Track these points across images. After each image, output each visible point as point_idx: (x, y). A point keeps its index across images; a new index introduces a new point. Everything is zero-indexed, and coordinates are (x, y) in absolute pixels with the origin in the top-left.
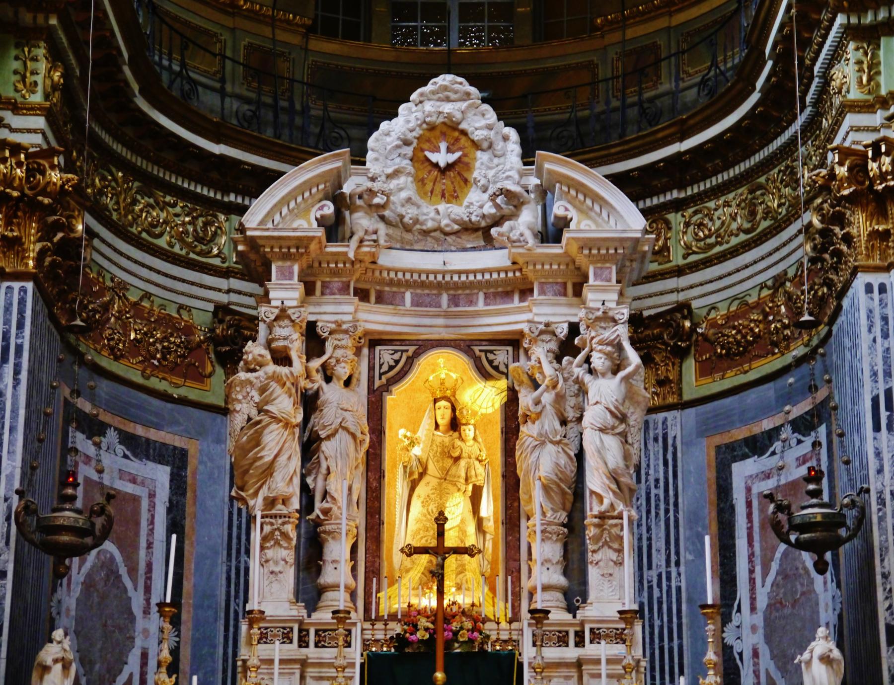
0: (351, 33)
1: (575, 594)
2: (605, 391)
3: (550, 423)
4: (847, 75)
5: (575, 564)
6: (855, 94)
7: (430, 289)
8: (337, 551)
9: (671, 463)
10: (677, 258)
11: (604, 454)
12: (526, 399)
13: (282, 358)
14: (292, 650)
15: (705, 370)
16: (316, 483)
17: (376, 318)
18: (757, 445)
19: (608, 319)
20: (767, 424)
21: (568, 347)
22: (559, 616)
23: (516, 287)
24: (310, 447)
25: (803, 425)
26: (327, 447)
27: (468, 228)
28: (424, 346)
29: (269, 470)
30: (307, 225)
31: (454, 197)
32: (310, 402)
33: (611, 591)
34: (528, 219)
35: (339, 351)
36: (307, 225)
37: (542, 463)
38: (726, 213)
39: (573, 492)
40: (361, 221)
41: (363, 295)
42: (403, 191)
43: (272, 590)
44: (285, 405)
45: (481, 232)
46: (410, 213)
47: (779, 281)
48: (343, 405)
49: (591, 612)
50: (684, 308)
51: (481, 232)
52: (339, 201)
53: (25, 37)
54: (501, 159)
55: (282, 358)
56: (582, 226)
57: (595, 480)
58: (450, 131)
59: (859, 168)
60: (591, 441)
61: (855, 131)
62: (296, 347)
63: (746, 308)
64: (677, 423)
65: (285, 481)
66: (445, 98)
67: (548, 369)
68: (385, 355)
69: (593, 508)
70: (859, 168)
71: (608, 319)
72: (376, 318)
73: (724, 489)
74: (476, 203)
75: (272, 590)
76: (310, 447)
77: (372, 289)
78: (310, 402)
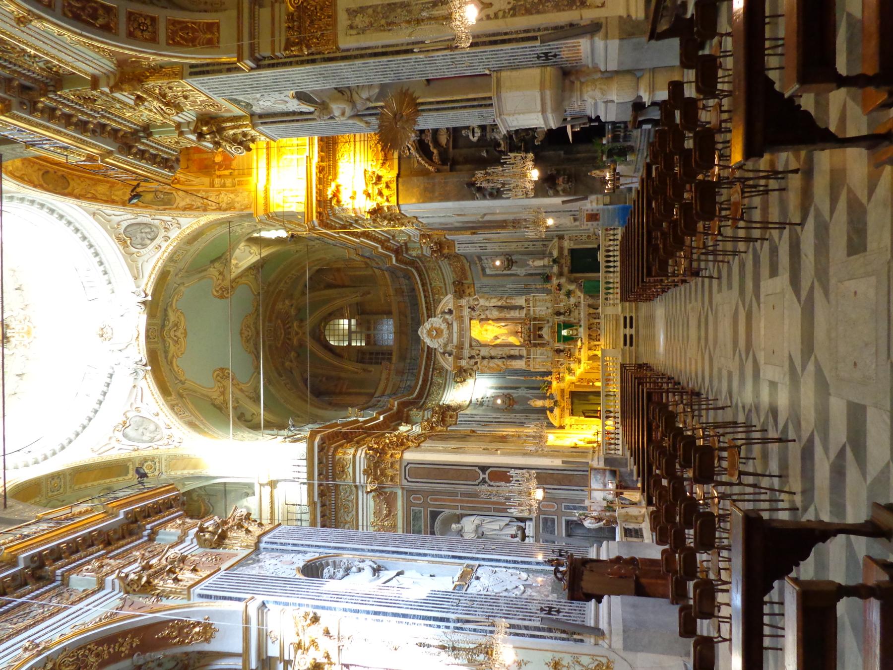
0: (391, 354)
1: (521, 308)
2: (482, 302)
3: (487, 312)
4: (414, 254)
5: (514, 308)
6: (419, 252)
7: (461, 336)
8: (512, 352)
9: (486, 286)
10: (442, 285)
11: (494, 302)
12: (483, 317)
13: (476, 363)
14: (531, 360)
15: (466, 279)
16: (499, 356)
17: (467, 345)
18: (483, 269)
19: (468, 301)
20: (479, 268)
21: (473, 309)
22: (525, 311)
23: (460, 319)
24: (492, 358)
25: (480, 259)
26: (493, 354)
27: (448, 328)
28: (471, 338)
29: (498, 366)
30: (451, 359)
31: (442, 331)
32: (483, 358)
33: (520, 301)
34: (447, 316)
35: (474, 353)
36: (451, 359)
37: (495, 314)
38: (433, 275)
39: (501, 308)
40: (449, 348)
41: (462, 348)
42: (441, 341)
43: (520, 364)
44: (485, 362)
45: (450, 325)
46: (446, 339)
47: (450, 264)
48: (484, 352)
49: (524, 304)
50: (454, 283)
51: (450, 325)
52: (444, 353)
53: (408, 416)
54: (436, 321)
55: (476, 363)
56: (451, 306)
57: (500, 304)
58: (429, 333)
59: (435, 252)
60: (492, 305)
61: (427, 252)
62: (473, 361)
63: (454, 271)
64: (477, 285)
65: (500, 362)
66: (423, 332)
67: (478, 313)
68: (474, 344)
69: (504, 304)
70: (435, 252)
71: (468, 301)
72: (467, 345)
73: (491, 276)
74: (444, 326)
75: (520, 364)
76: (492, 358)
77: (460, 347)
78: (483, 358)
